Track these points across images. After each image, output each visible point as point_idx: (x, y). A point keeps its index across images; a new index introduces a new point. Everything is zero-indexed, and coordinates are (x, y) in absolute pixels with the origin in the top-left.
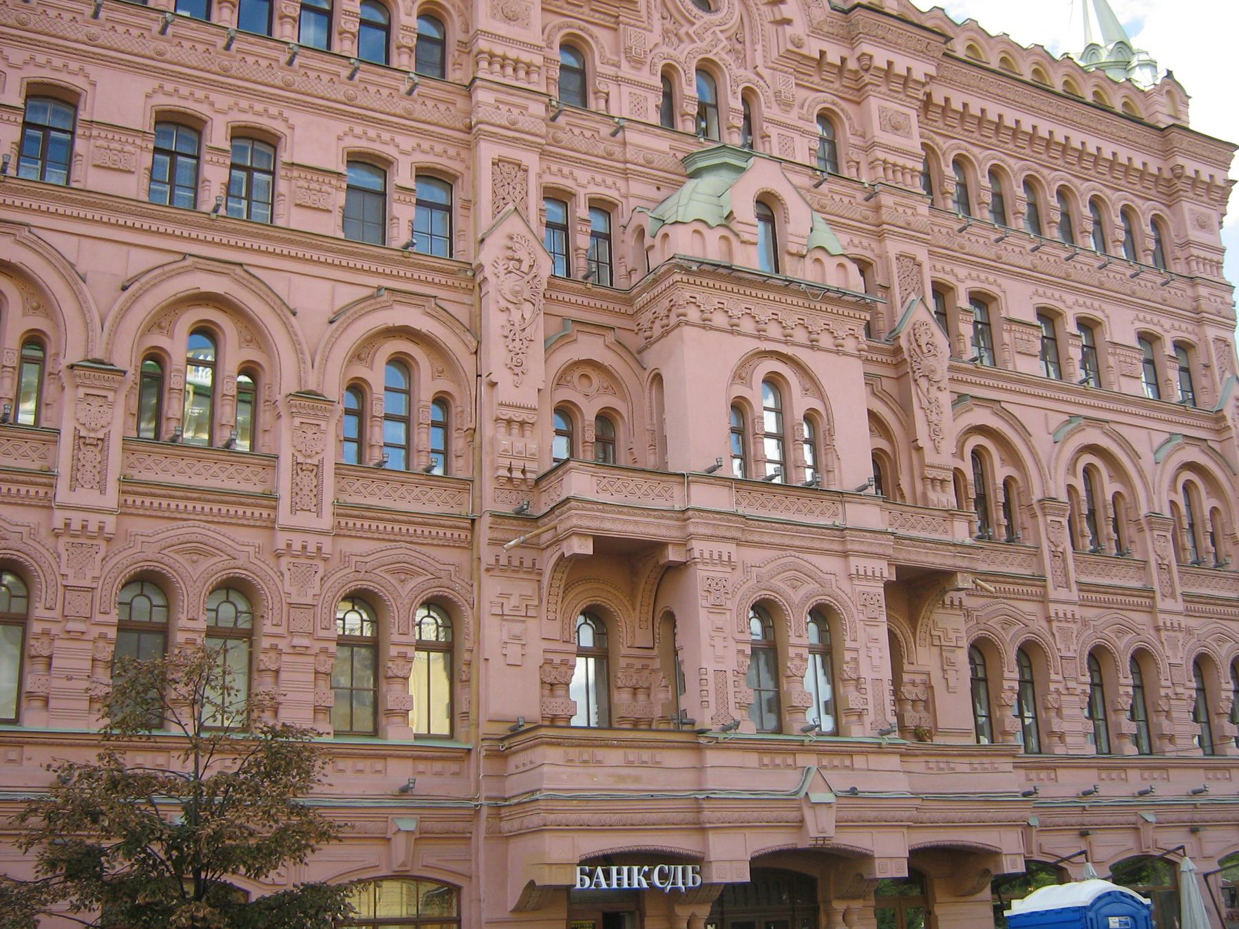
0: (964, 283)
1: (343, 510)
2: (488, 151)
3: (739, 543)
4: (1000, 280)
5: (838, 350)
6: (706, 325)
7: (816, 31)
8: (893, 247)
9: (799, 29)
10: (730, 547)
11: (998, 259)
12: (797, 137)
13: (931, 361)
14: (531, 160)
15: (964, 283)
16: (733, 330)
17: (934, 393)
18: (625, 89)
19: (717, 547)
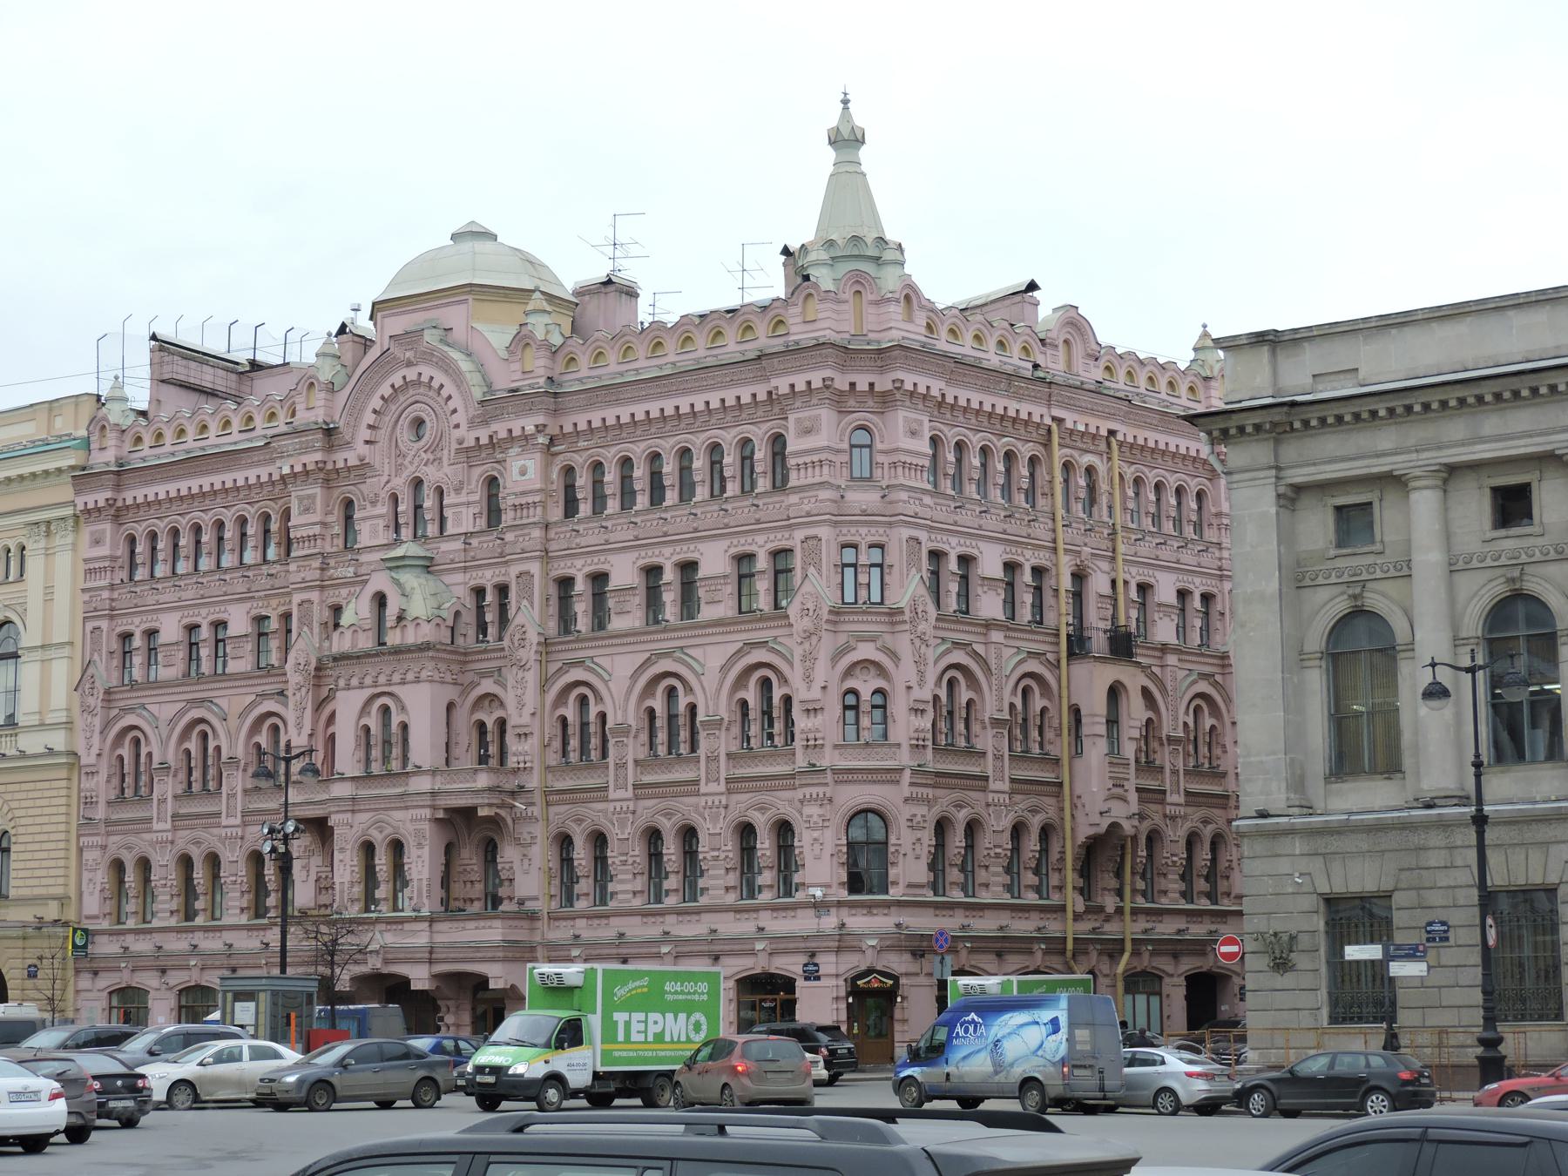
0: (579, 570)
1: (244, 814)
2: (297, 598)
3: (353, 811)
4: (612, 558)
5: (417, 680)
6: (348, 687)
7: (472, 424)
8: (514, 570)
9: (464, 426)
10: (349, 815)
11: (607, 542)
12: (463, 509)
13: (522, 653)
14: (314, 596)
15: (579, 570)
16: (361, 686)
17: (520, 674)
18: (369, 523)
19: (341, 816)
